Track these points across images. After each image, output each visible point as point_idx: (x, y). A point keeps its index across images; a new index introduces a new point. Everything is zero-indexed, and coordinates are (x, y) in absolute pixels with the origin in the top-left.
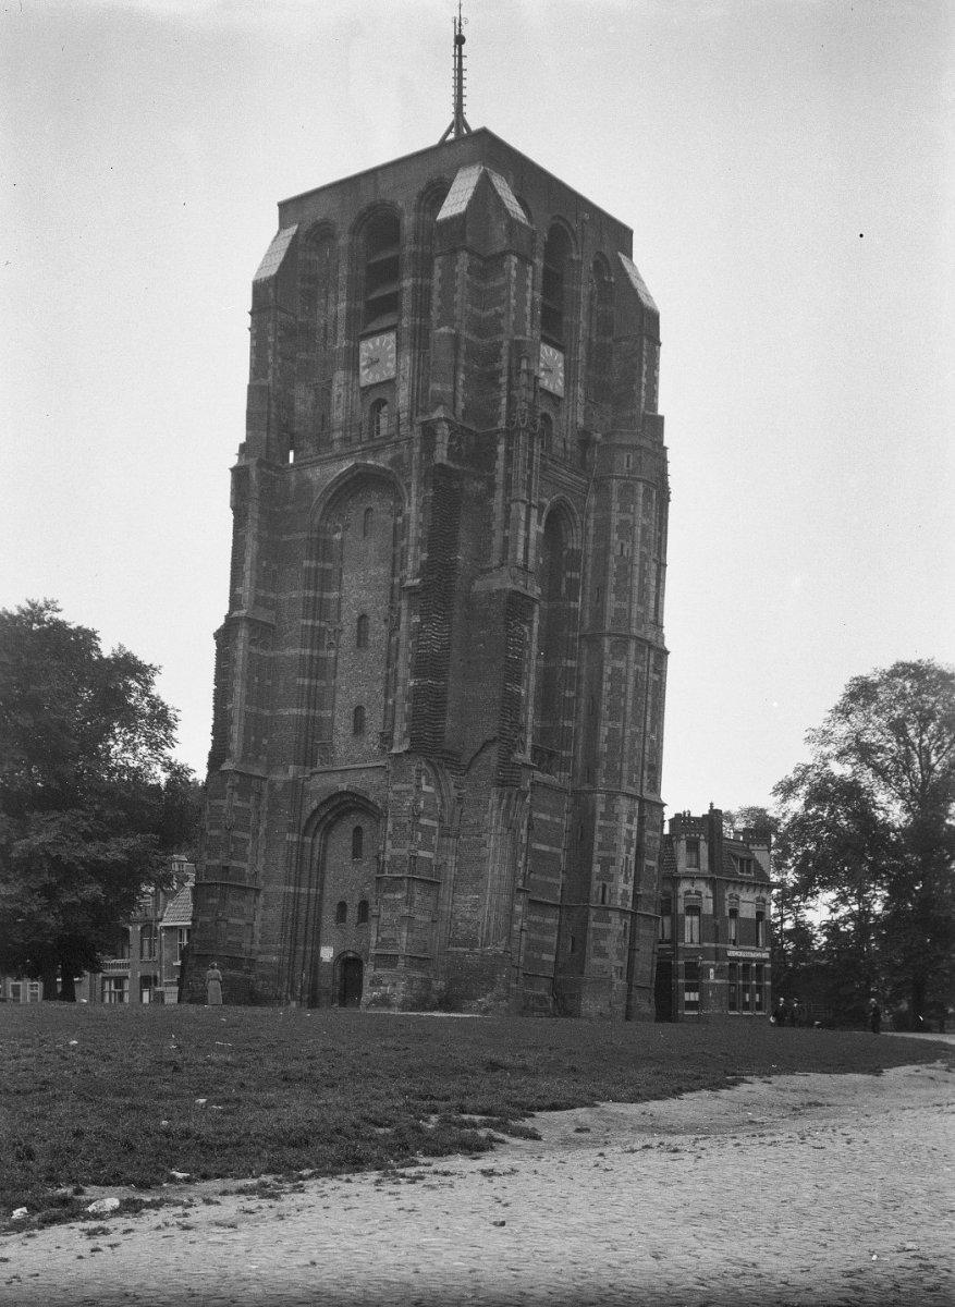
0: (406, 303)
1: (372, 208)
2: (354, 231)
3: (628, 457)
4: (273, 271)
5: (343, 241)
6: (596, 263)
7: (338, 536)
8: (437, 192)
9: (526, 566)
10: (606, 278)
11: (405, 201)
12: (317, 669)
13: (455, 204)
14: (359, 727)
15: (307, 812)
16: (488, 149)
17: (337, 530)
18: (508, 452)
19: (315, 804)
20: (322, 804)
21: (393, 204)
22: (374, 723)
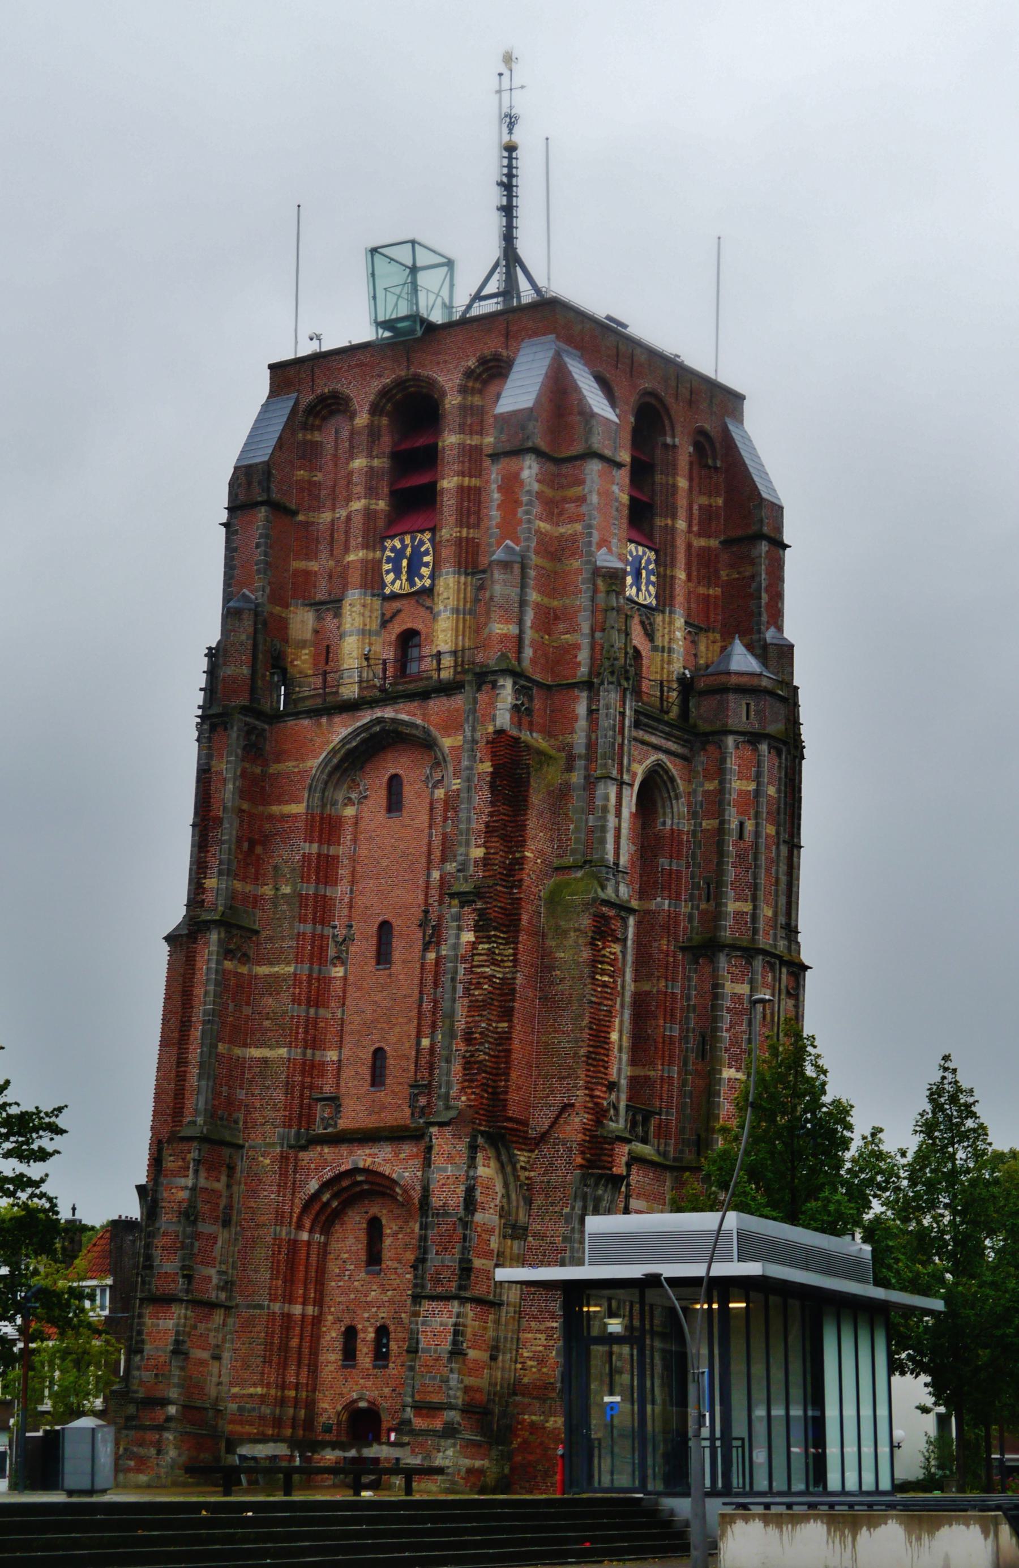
0: (448, 504)
1: (400, 384)
2: (375, 410)
3: (748, 705)
4: (262, 455)
5: (362, 419)
6: (698, 446)
7: (350, 811)
8: (494, 370)
9: (617, 864)
10: (710, 462)
11: (448, 380)
12: (316, 993)
13: (520, 392)
14: (377, 1076)
15: (302, 1196)
16: (553, 317)
17: (349, 802)
18: (591, 712)
19: (313, 1186)
20: (325, 1186)
21: (432, 383)
22: (400, 1071)
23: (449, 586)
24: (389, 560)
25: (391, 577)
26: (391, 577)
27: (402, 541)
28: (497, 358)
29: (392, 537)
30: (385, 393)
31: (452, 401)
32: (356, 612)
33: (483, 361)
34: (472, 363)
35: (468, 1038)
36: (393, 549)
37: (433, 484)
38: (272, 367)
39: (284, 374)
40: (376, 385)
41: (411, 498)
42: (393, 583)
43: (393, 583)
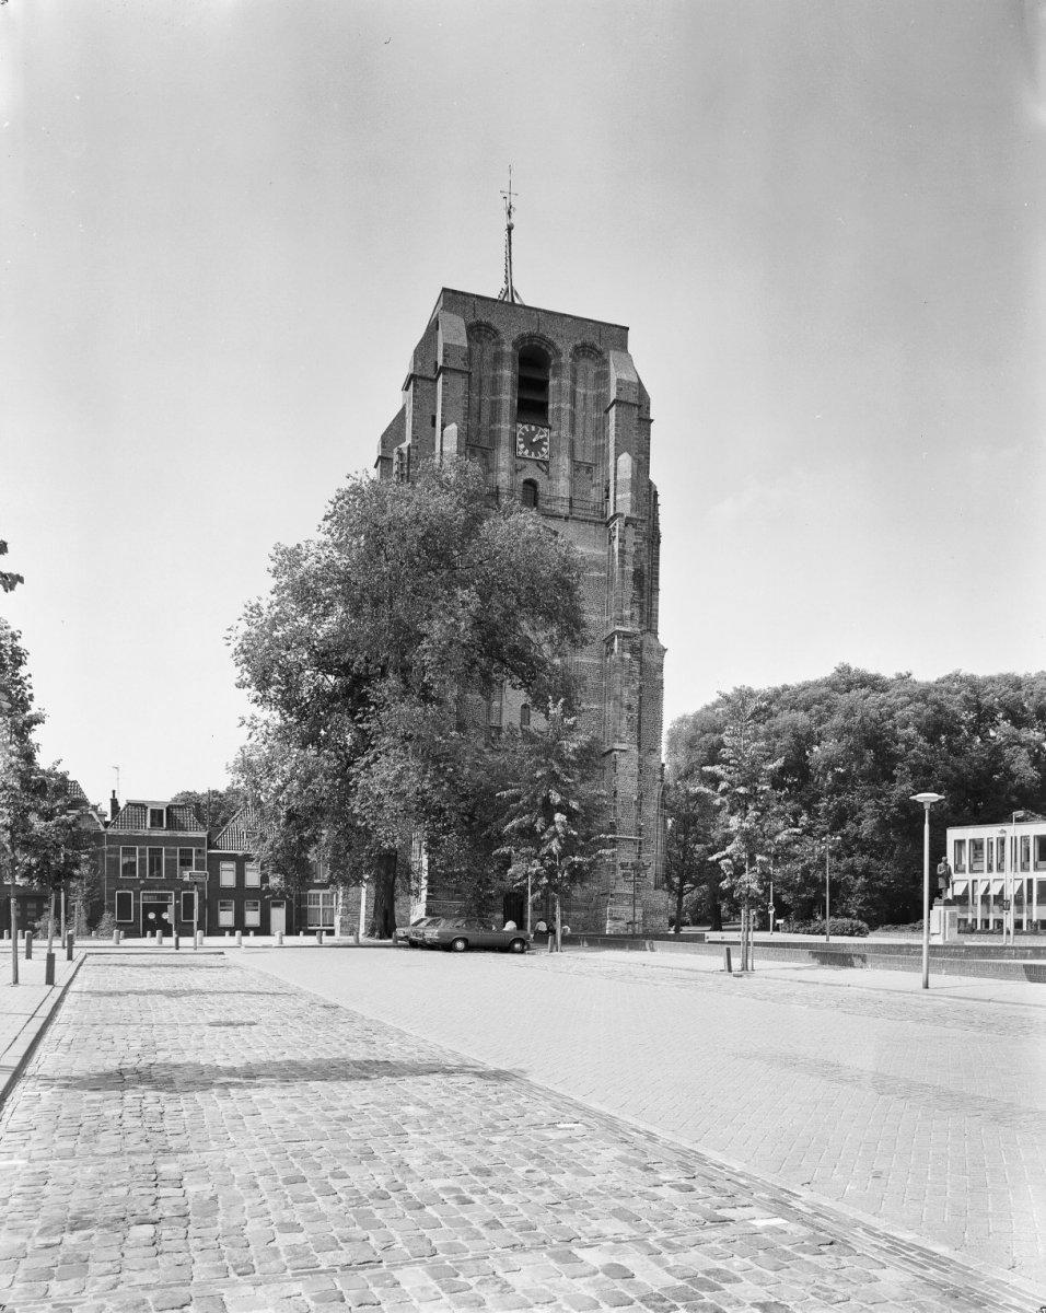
1: (531, 337)
2: (515, 344)
5: (508, 348)
11: (566, 348)
21: (551, 344)
23: (564, 463)
24: (521, 436)
25: (522, 446)
26: (522, 446)
27: (530, 428)
28: (593, 347)
29: (523, 424)
30: (522, 338)
31: (566, 359)
32: (503, 459)
33: (584, 345)
34: (579, 342)
35: (629, 708)
36: (524, 430)
37: (547, 404)
38: (445, 290)
39: (452, 299)
40: (515, 333)
41: (532, 406)
42: (524, 450)
43: (524, 450)
